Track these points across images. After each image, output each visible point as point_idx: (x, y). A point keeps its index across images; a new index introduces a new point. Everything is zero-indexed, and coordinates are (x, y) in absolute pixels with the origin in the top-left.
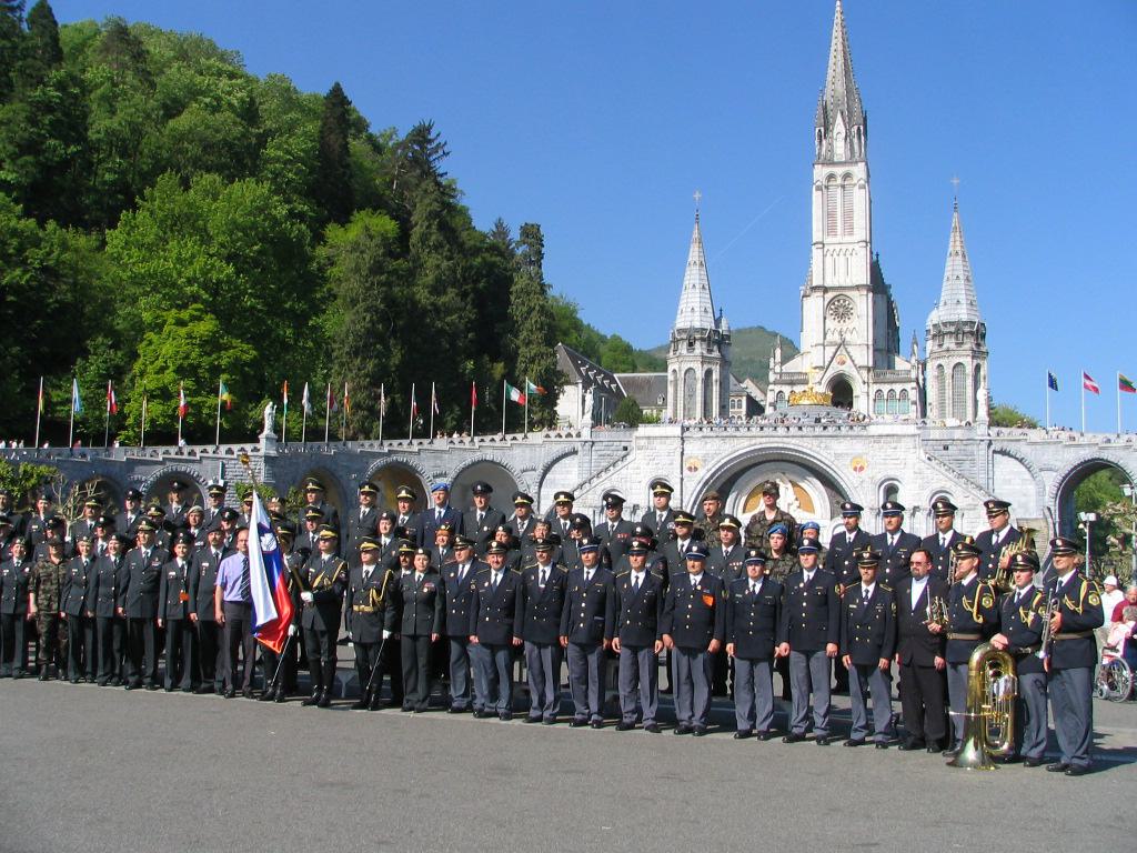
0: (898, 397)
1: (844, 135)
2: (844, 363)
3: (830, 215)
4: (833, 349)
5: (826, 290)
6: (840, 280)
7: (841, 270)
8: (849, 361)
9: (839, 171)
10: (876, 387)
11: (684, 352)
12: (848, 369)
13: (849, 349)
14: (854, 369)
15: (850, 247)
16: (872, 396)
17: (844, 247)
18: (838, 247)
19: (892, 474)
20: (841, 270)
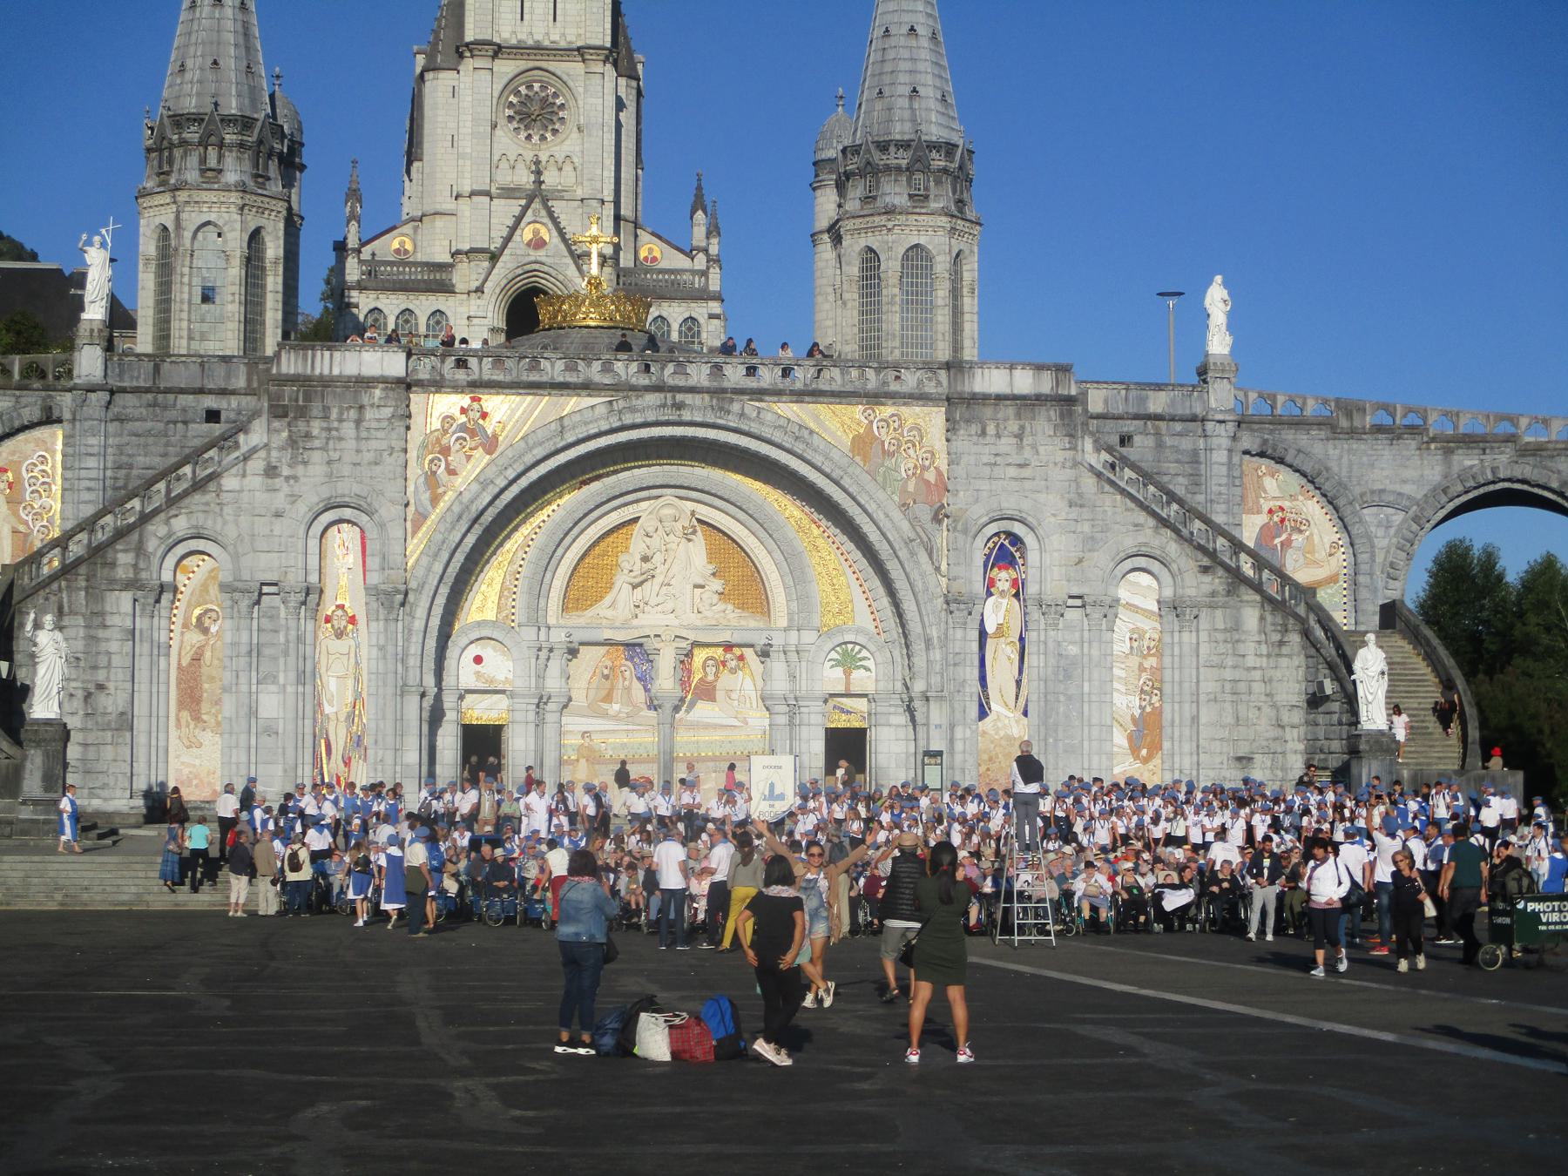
4: (515, 207)
5: (498, 51)
6: (538, 29)
11: (192, 176)
13: (558, 207)
14: (569, 261)
19: (1010, 505)
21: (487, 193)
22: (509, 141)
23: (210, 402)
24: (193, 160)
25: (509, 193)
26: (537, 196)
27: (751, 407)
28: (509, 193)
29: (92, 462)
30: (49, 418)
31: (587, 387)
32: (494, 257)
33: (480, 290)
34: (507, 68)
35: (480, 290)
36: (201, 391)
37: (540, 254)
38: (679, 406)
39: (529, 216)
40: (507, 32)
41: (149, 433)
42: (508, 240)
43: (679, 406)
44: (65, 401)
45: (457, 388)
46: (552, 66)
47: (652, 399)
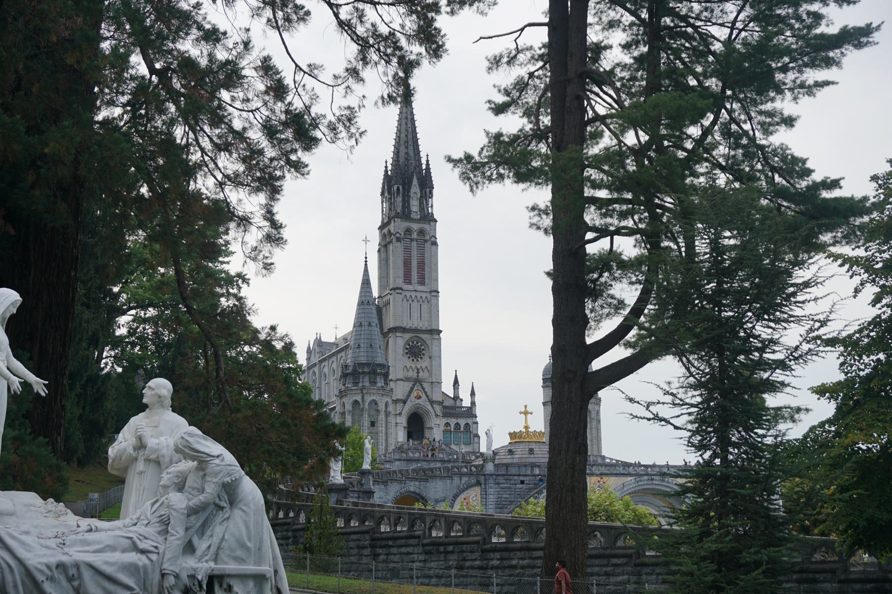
0: (462, 429)
1: (419, 196)
2: (419, 397)
3: (407, 264)
4: (410, 384)
5: (404, 330)
6: (416, 323)
7: (415, 315)
8: (424, 396)
9: (415, 226)
10: (445, 421)
11: (367, 384)
12: (423, 402)
13: (425, 385)
15: (424, 295)
16: (442, 428)
17: (419, 295)
18: (413, 294)
20: (415, 315)
21: (401, 380)
22: (408, 363)
23: (522, 478)
24: (367, 379)
25: (407, 379)
26: (417, 381)
27: (670, 479)
28: (407, 379)
29: (492, 497)
30: (478, 483)
31: (630, 475)
32: (405, 402)
33: (400, 414)
34: (407, 336)
35: (400, 414)
36: (519, 475)
37: (419, 401)
38: (652, 479)
39: (416, 388)
40: (407, 323)
41: (506, 488)
42: (409, 395)
43: (652, 479)
44: (482, 478)
45: (597, 475)
46: (422, 336)
47: (645, 478)
